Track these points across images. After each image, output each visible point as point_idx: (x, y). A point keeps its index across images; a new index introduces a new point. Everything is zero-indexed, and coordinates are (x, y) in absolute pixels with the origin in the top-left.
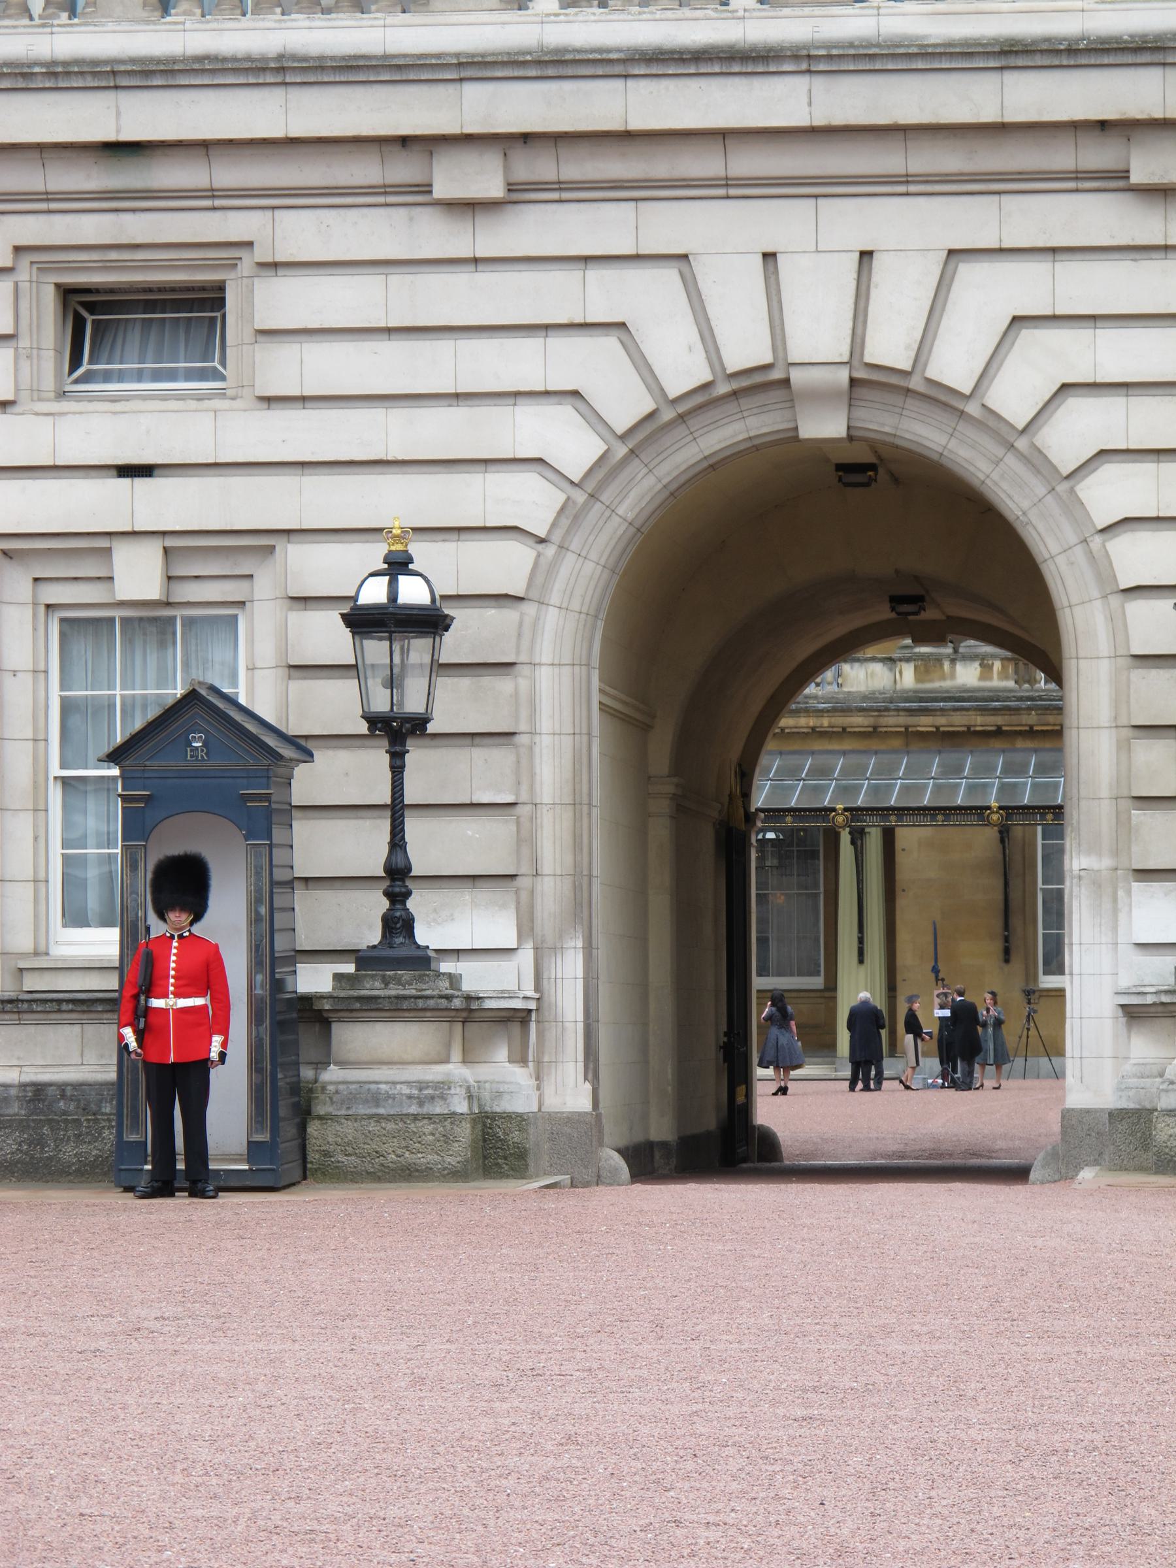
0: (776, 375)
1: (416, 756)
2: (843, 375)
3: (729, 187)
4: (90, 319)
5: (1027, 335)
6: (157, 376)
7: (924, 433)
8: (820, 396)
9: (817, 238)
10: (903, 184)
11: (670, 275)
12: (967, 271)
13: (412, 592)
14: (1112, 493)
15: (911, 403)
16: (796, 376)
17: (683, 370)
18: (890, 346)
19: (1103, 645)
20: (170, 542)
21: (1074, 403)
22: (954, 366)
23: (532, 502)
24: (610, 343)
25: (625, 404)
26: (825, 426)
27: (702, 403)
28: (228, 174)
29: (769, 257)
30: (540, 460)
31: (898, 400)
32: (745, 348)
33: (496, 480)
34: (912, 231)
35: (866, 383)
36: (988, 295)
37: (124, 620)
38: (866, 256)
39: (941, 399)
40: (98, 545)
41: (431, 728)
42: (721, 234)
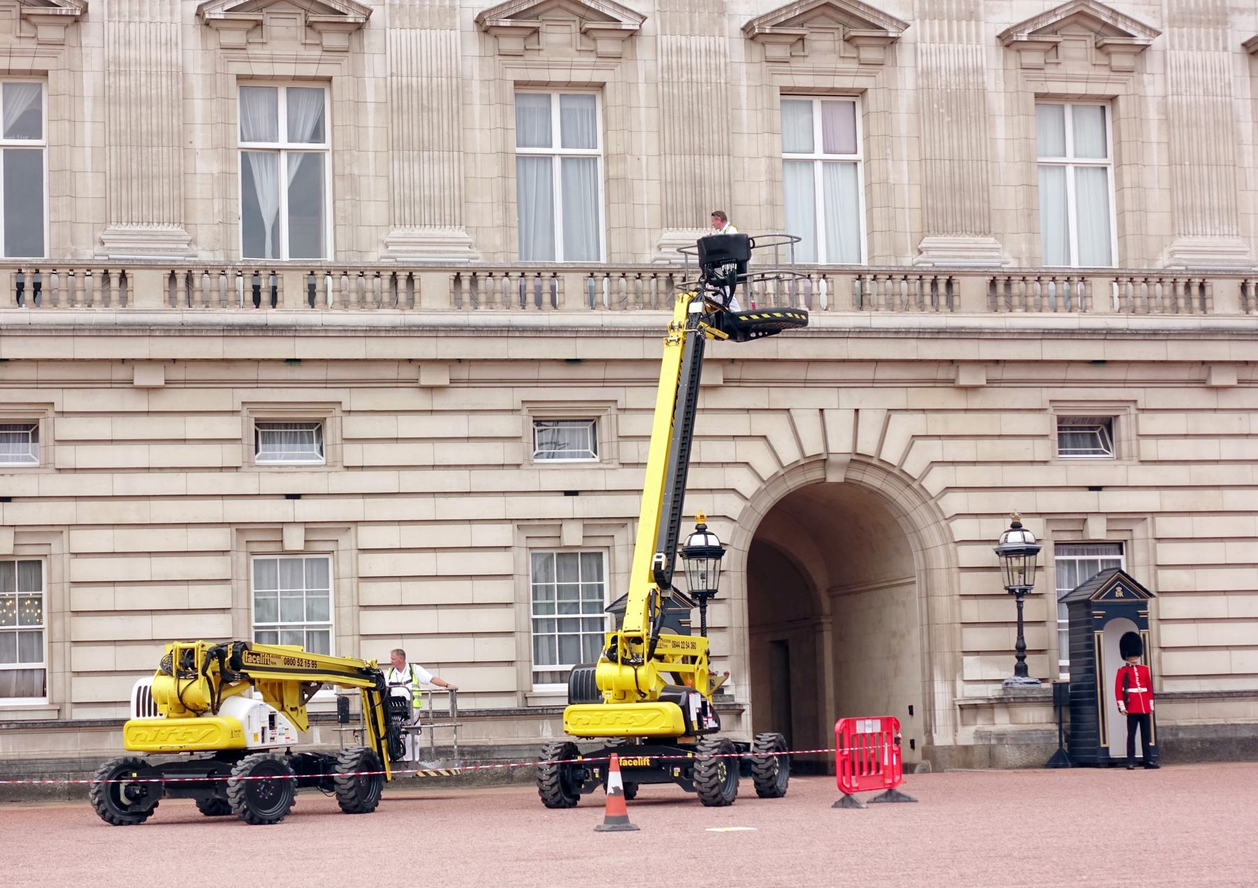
0: (824, 457)
1: (711, 608)
2: (848, 458)
3: (806, 383)
4: (260, 431)
5: (918, 443)
6: (1076, 453)
7: (872, 480)
8: (840, 466)
9: (839, 403)
10: (873, 383)
11: (783, 418)
12: (895, 417)
13: (713, 541)
14: (954, 503)
15: (869, 469)
16: (832, 458)
17: (790, 455)
18: (867, 446)
19: (943, 564)
20: (586, 522)
21: (937, 470)
22: (891, 454)
23: (733, 506)
24: (761, 444)
25: (767, 468)
26: (834, 477)
27: (796, 467)
28: (612, 373)
29: (821, 410)
30: (734, 490)
31: (863, 467)
32: (813, 447)
33: (718, 497)
34: (873, 402)
35: (859, 460)
36: (902, 427)
37: (559, 554)
38: (857, 410)
39: (885, 468)
40: (558, 523)
41: (716, 596)
42: (804, 402)
